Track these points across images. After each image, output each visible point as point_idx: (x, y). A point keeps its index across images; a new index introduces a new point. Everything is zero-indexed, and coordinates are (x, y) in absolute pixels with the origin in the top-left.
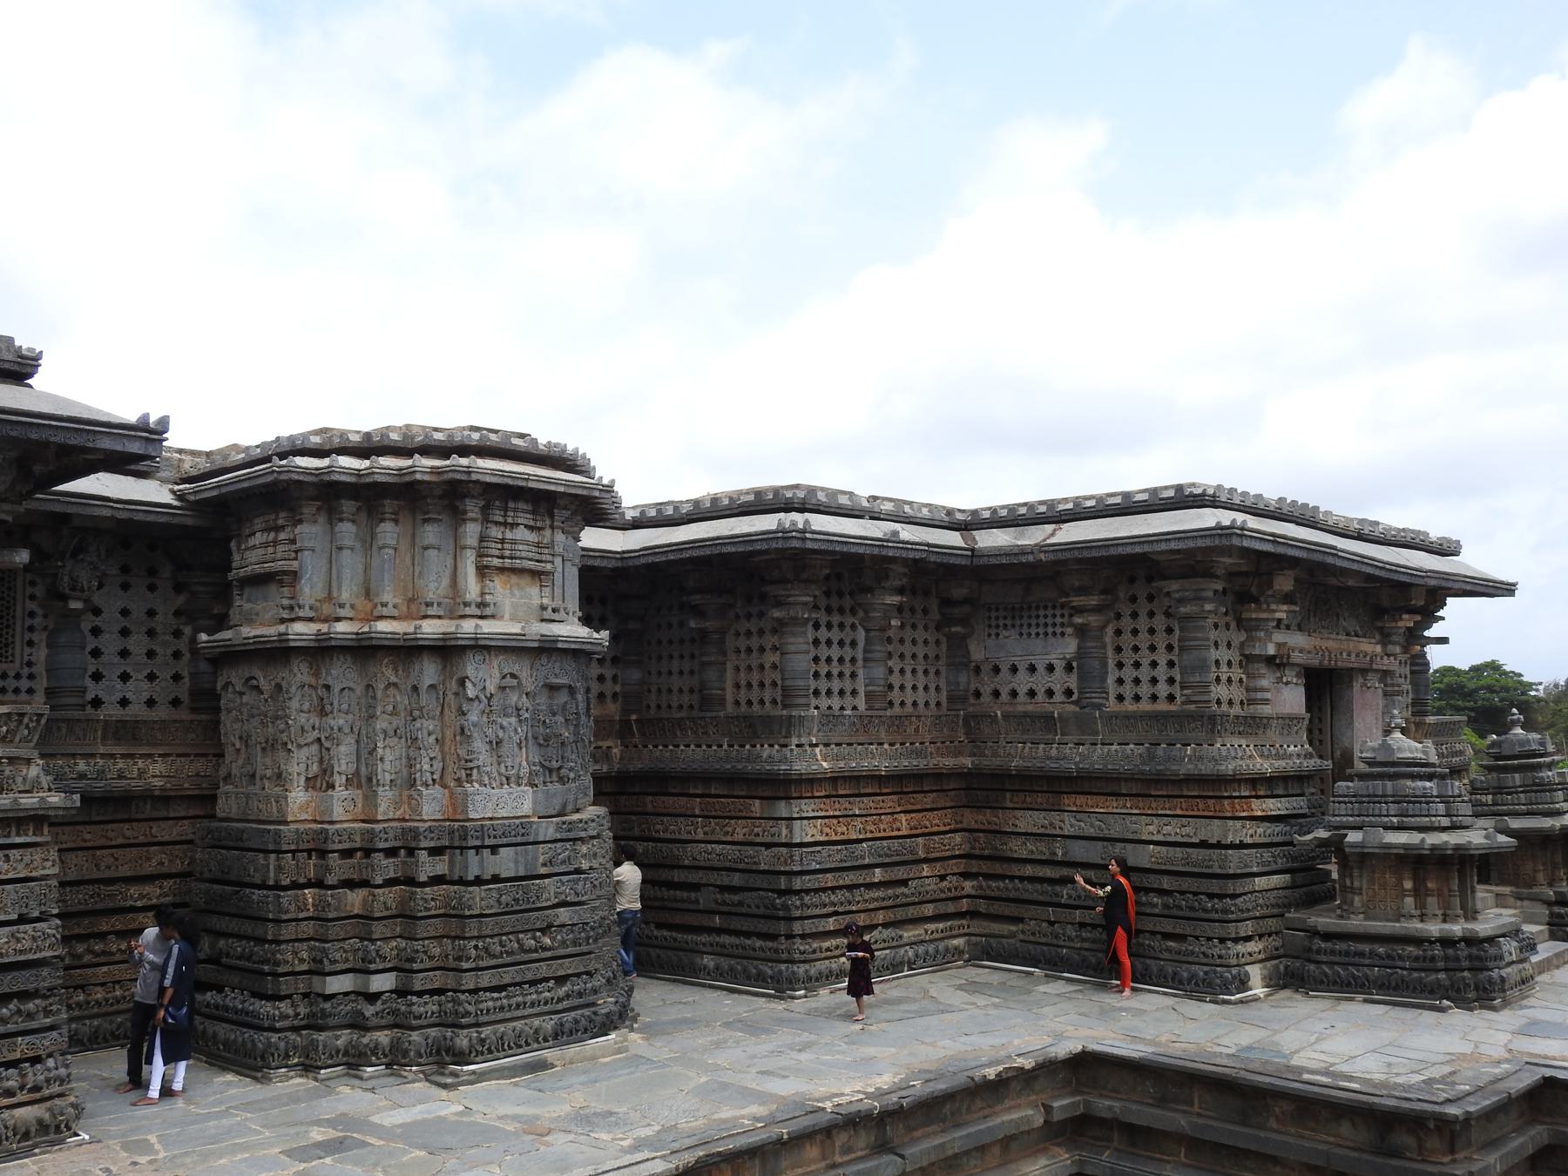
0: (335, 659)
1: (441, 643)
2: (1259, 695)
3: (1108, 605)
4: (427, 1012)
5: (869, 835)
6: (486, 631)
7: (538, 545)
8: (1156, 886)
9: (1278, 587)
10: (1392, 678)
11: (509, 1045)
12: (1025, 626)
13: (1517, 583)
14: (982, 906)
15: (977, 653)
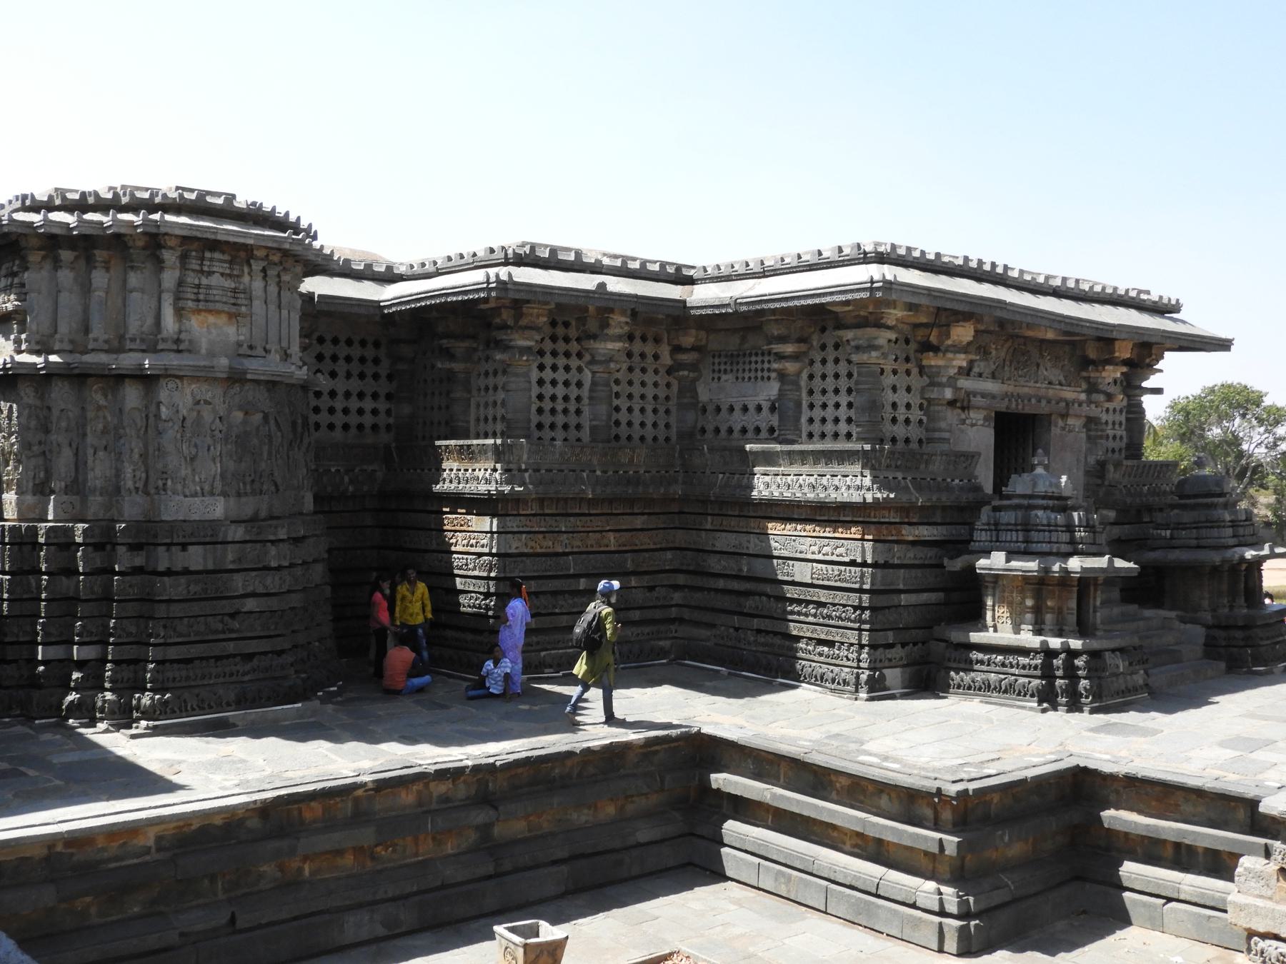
0: (53, 385)
1: (139, 373)
2: (937, 435)
3: (804, 352)
4: (123, 678)
5: (575, 550)
6: (175, 363)
7: (234, 291)
8: (815, 599)
9: (956, 338)
10: (1096, 424)
11: (192, 706)
12: (741, 371)
13: (1233, 339)
14: (686, 614)
15: (704, 395)
